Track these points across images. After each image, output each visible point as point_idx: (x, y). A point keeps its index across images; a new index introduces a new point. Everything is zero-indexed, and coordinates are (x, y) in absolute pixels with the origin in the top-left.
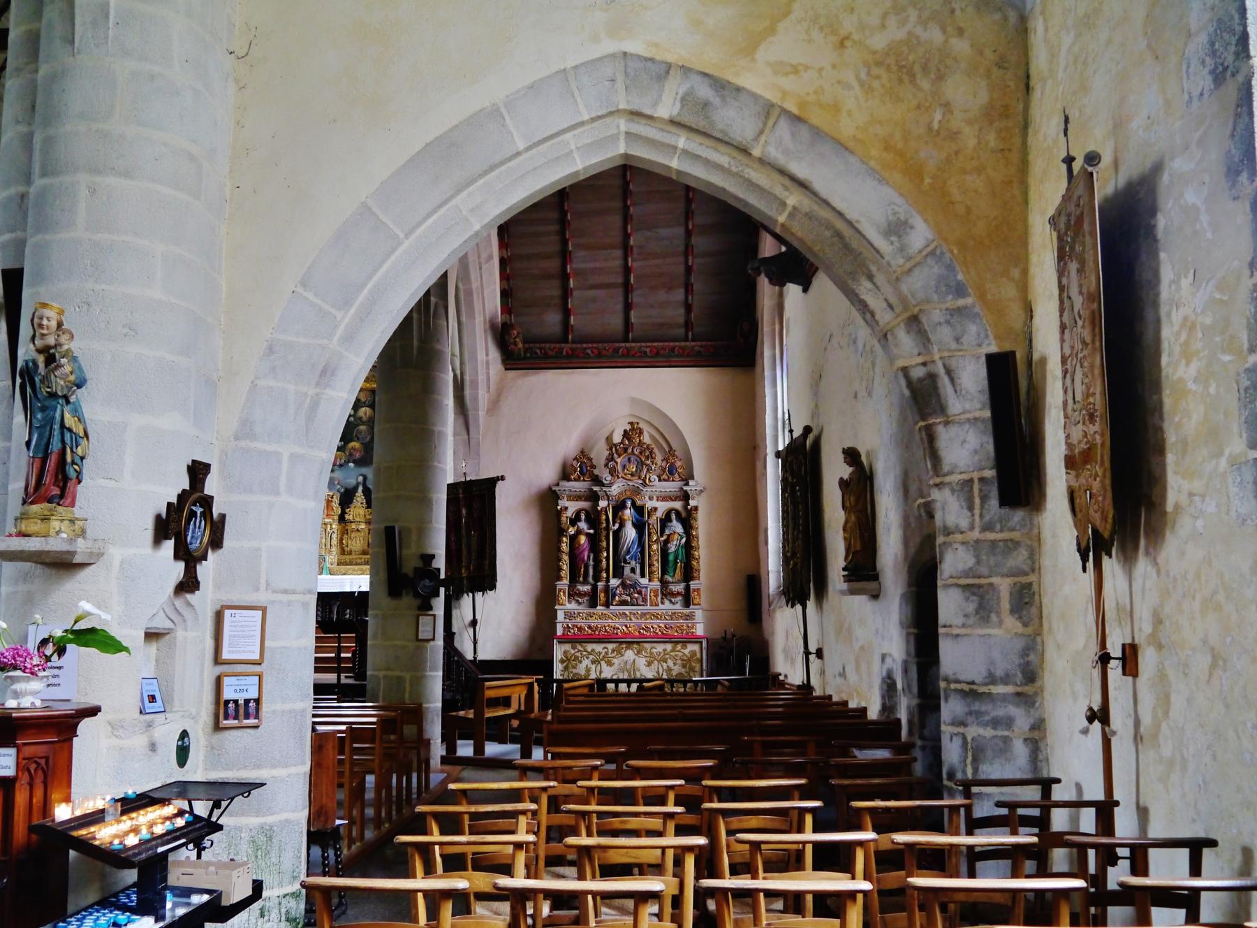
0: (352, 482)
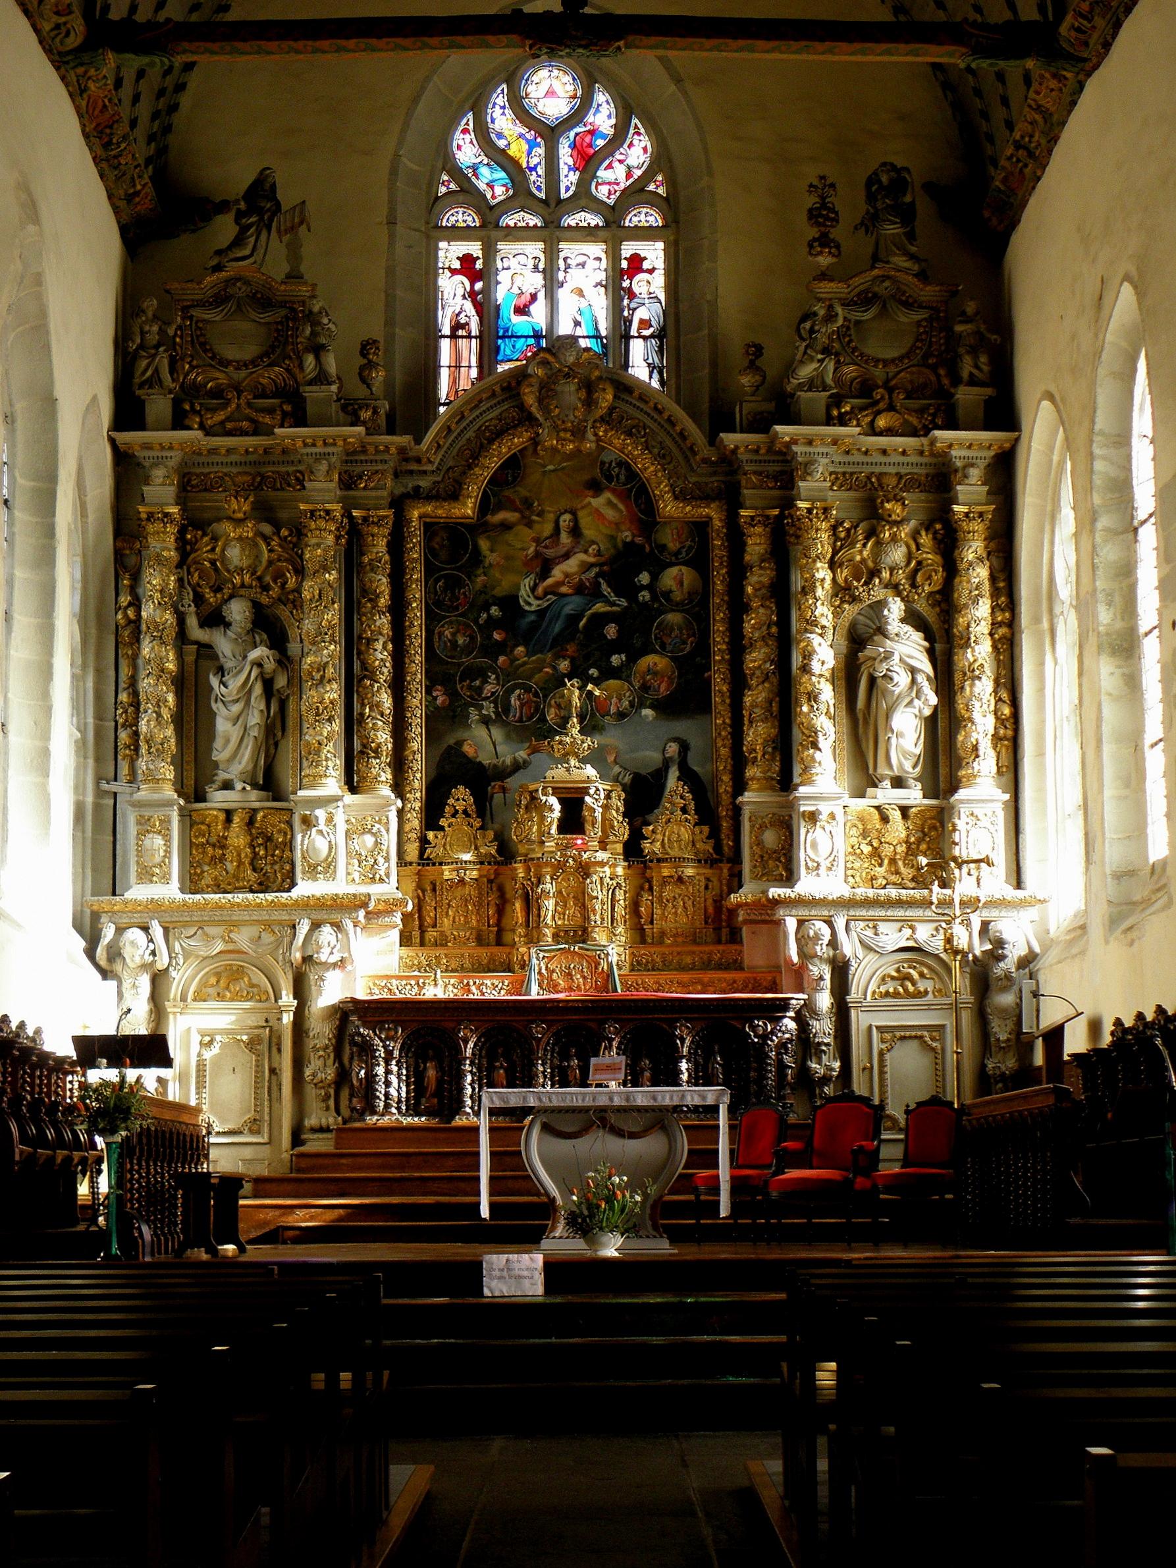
0: (651, 757)
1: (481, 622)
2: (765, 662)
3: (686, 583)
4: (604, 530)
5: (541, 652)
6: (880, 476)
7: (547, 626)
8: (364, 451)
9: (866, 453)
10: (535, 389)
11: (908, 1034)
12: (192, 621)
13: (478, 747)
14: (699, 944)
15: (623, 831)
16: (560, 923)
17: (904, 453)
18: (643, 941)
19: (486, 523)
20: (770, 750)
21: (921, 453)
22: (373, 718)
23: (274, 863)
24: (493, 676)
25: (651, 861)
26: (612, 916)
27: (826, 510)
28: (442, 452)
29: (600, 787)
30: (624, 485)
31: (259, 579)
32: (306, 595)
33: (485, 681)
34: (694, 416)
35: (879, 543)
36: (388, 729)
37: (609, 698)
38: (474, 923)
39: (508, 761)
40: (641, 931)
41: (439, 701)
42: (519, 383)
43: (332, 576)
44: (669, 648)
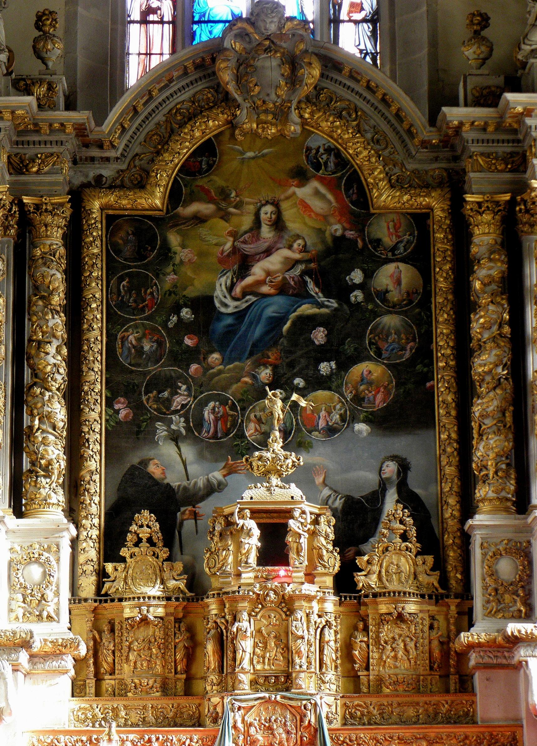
1: (170, 325)
2: (497, 366)
3: (404, 281)
4: (311, 223)
5: (239, 359)
7: (247, 330)
8: (37, 131)
10: (233, 63)
13: (166, 467)
14: (424, 694)
16: (259, 667)
18: (357, 690)
19: (177, 216)
20: (504, 466)
22: (43, 431)
24: (184, 387)
25: (366, 596)
26: (321, 660)
29: (308, 509)
30: (334, 173)
33: (175, 392)
34: (410, 91)
36: (61, 444)
38: (159, 669)
39: (201, 483)
41: (122, 414)
42: (213, 60)
44: (385, 355)
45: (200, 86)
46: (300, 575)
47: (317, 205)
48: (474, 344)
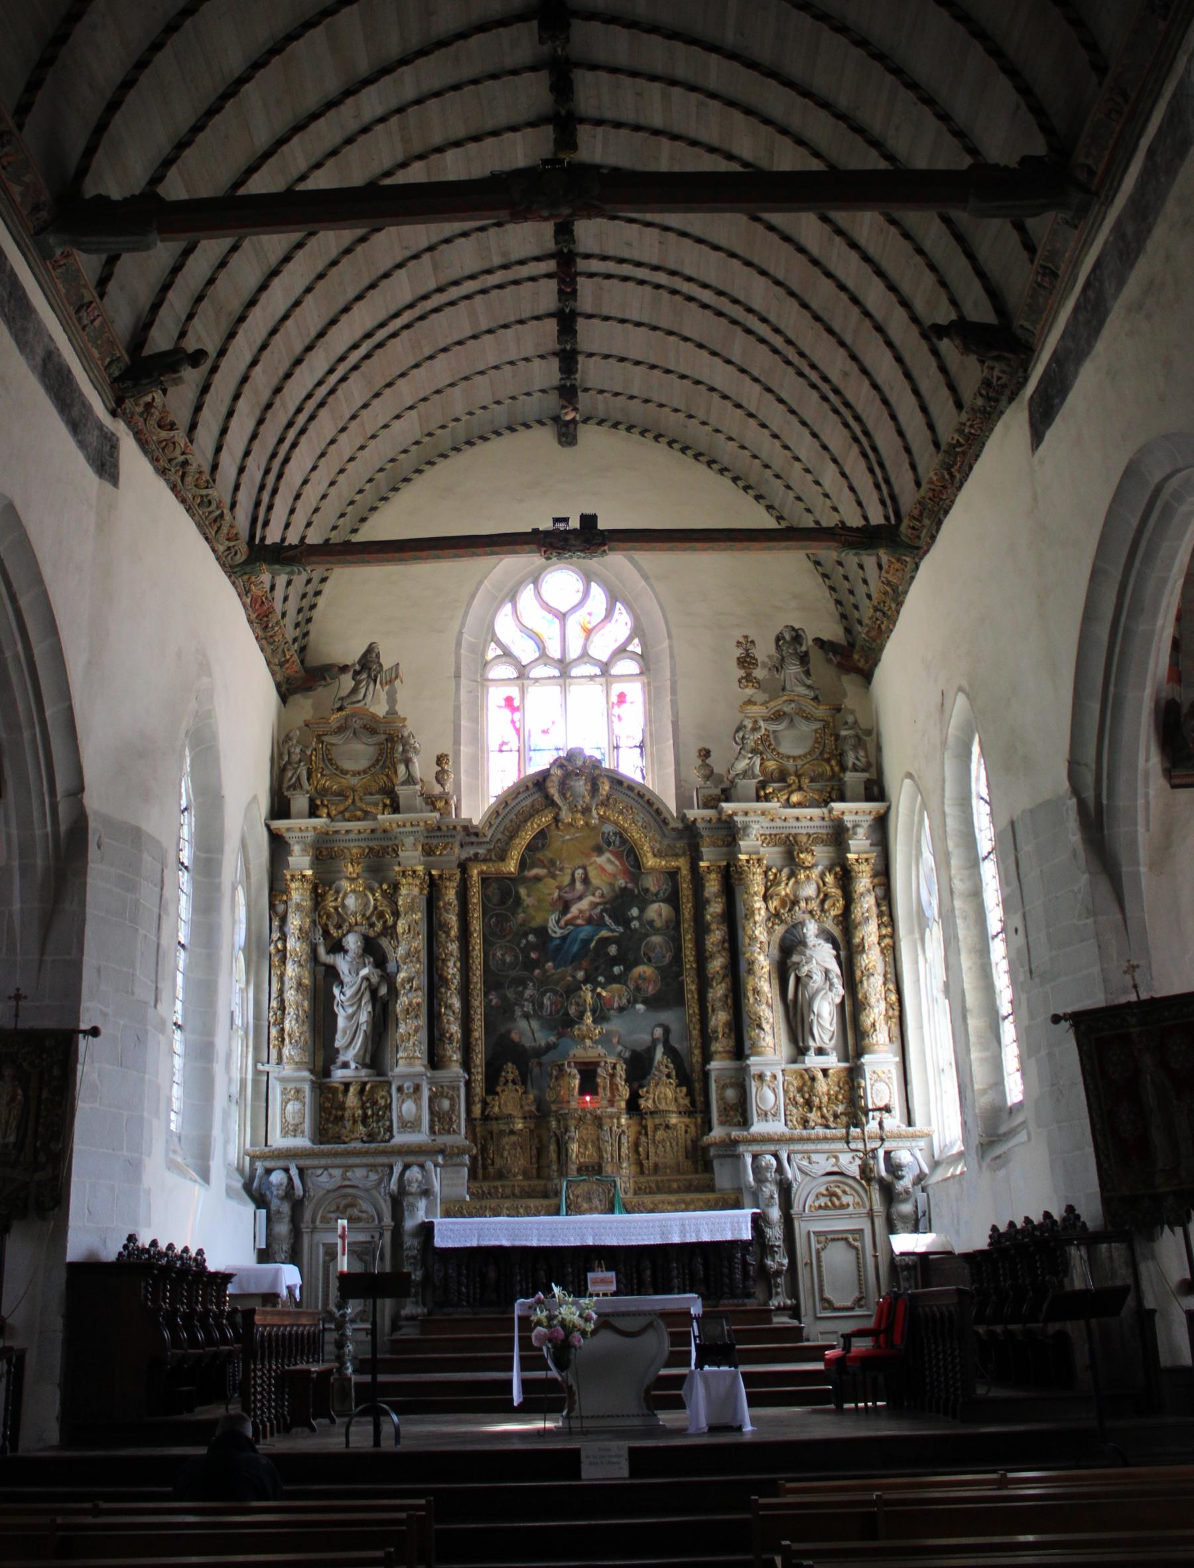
0: (642, 1038)
6: (795, 836)
9: (785, 820)
11: (836, 1236)
12: (322, 950)
13: (521, 1034)
14: (683, 1174)
15: (625, 1092)
17: (811, 819)
18: (642, 1172)
21: (823, 819)
23: (378, 1121)
27: (759, 860)
28: (493, 828)
31: (368, 919)
32: (400, 930)
33: (525, 987)
35: (797, 882)
37: (613, 997)
39: (543, 1043)
40: (640, 1164)
41: (494, 1002)
43: (418, 916)
45: (536, 796)
46: (605, 1103)
47: (609, 868)
48: (707, 954)
